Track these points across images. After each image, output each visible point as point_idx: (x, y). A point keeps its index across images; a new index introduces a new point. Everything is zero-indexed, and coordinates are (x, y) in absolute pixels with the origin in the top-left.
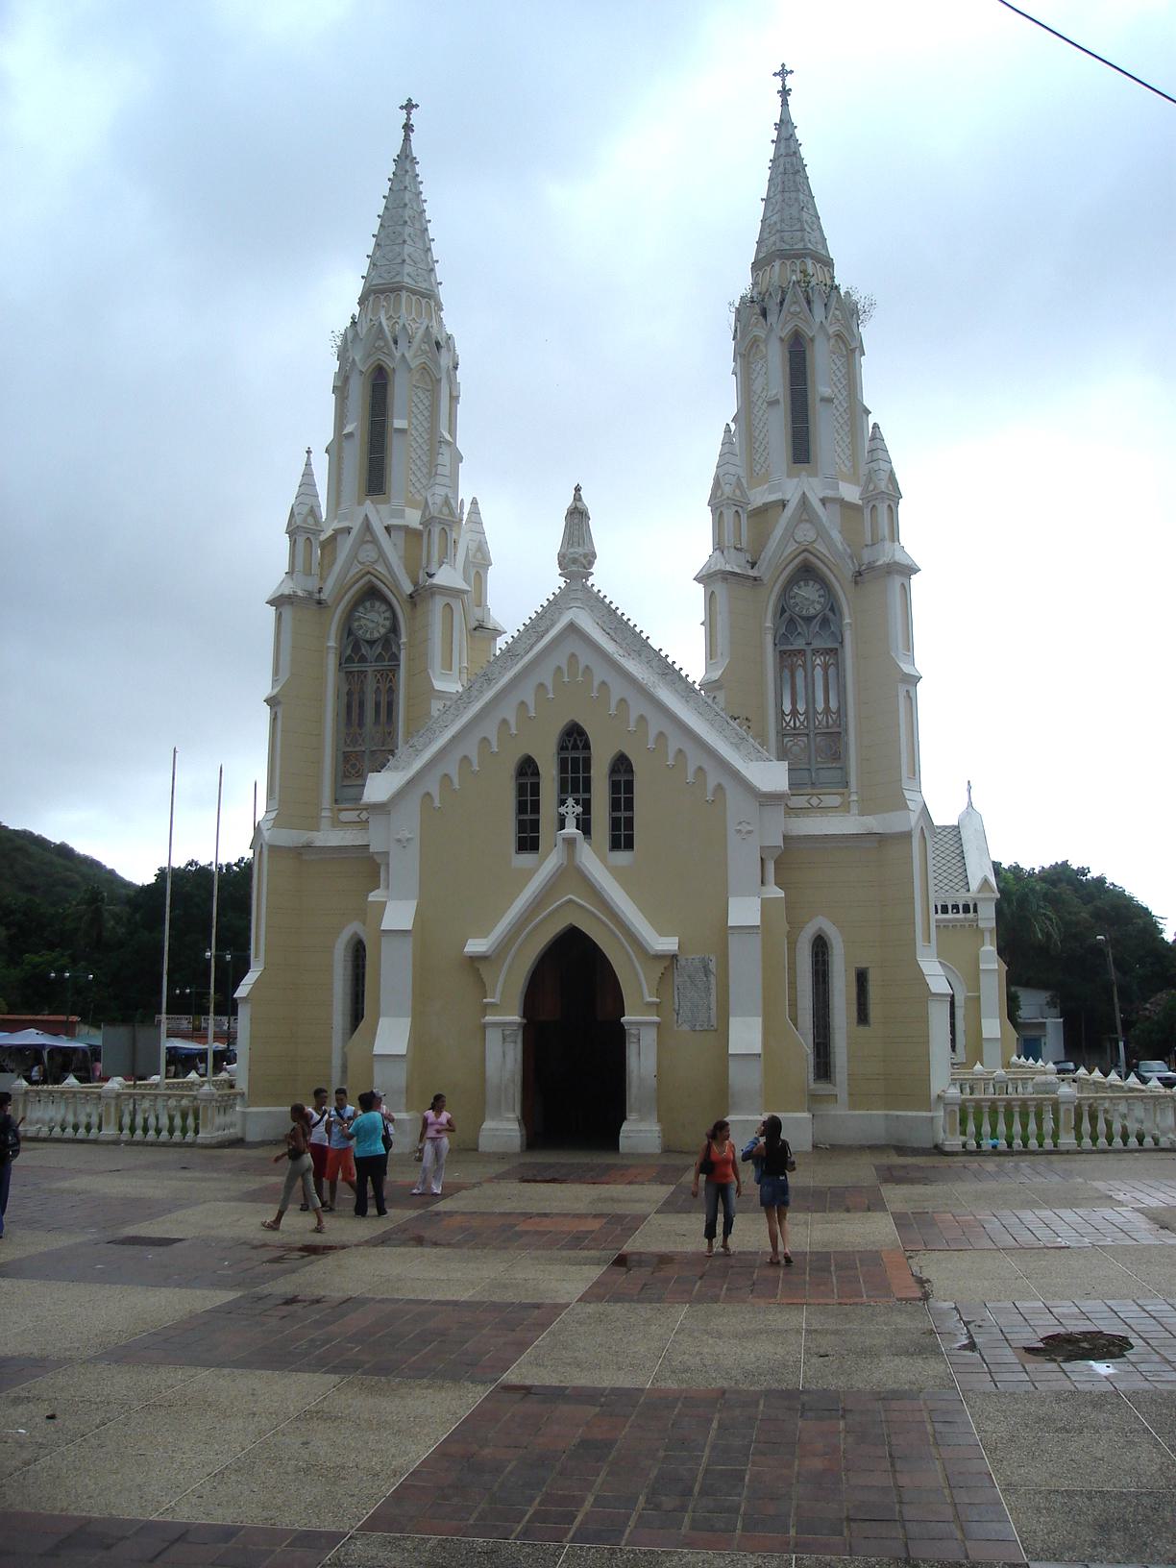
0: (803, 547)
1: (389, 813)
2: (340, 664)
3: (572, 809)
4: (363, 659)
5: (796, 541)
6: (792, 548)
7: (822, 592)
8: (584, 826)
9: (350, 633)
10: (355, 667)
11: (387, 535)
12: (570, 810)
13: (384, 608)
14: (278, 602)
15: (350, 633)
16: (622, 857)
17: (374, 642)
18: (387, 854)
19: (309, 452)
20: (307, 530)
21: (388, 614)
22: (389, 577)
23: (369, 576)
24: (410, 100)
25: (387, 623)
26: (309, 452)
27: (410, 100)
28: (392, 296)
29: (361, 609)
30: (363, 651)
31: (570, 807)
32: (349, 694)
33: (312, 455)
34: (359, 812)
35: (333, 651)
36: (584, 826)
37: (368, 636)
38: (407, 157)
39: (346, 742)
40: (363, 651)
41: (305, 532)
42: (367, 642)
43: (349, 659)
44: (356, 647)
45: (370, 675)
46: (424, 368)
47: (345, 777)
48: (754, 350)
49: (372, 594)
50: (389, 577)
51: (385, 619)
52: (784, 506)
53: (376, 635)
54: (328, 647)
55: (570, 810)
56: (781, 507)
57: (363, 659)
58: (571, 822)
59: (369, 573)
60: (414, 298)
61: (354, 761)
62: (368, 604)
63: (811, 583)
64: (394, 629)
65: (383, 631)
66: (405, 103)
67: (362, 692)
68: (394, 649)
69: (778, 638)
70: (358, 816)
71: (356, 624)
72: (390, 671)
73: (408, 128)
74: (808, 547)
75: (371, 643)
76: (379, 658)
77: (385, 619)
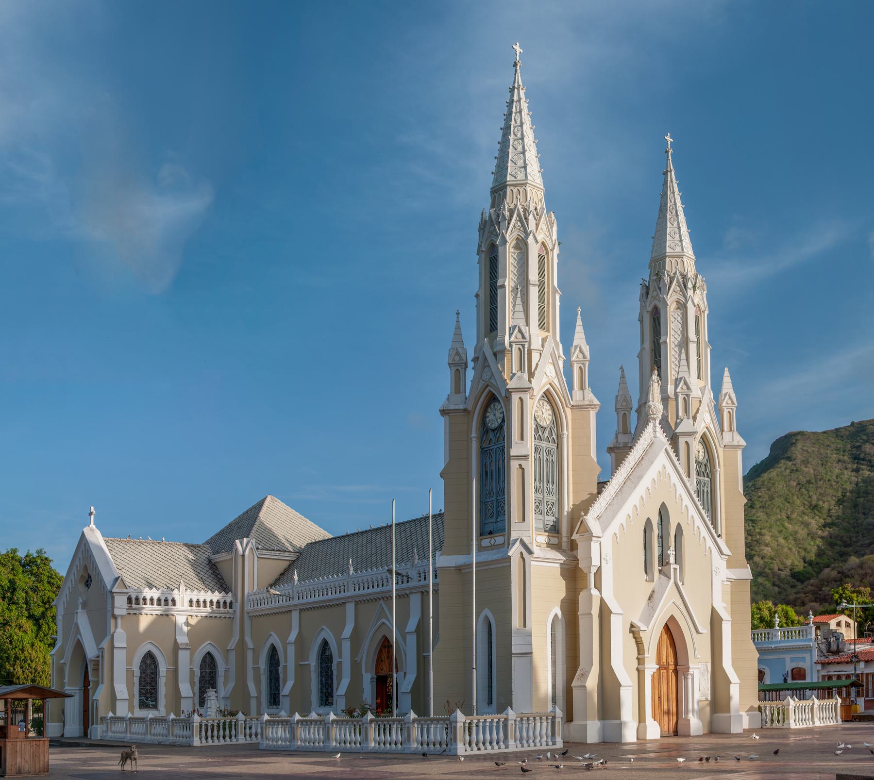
11: (495, 360)
14: (444, 412)
19: (458, 314)
23: (489, 387)
25: (501, 416)
26: (458, 314)
29: (489, 410)
33: (459, 316)
37: (493, 427)
40: (491, 437)
49: (492, 399)
53: (497, 425)
61: (489, 507)
64: (503, 421)
65: (500, 421)
75: (493, 430)
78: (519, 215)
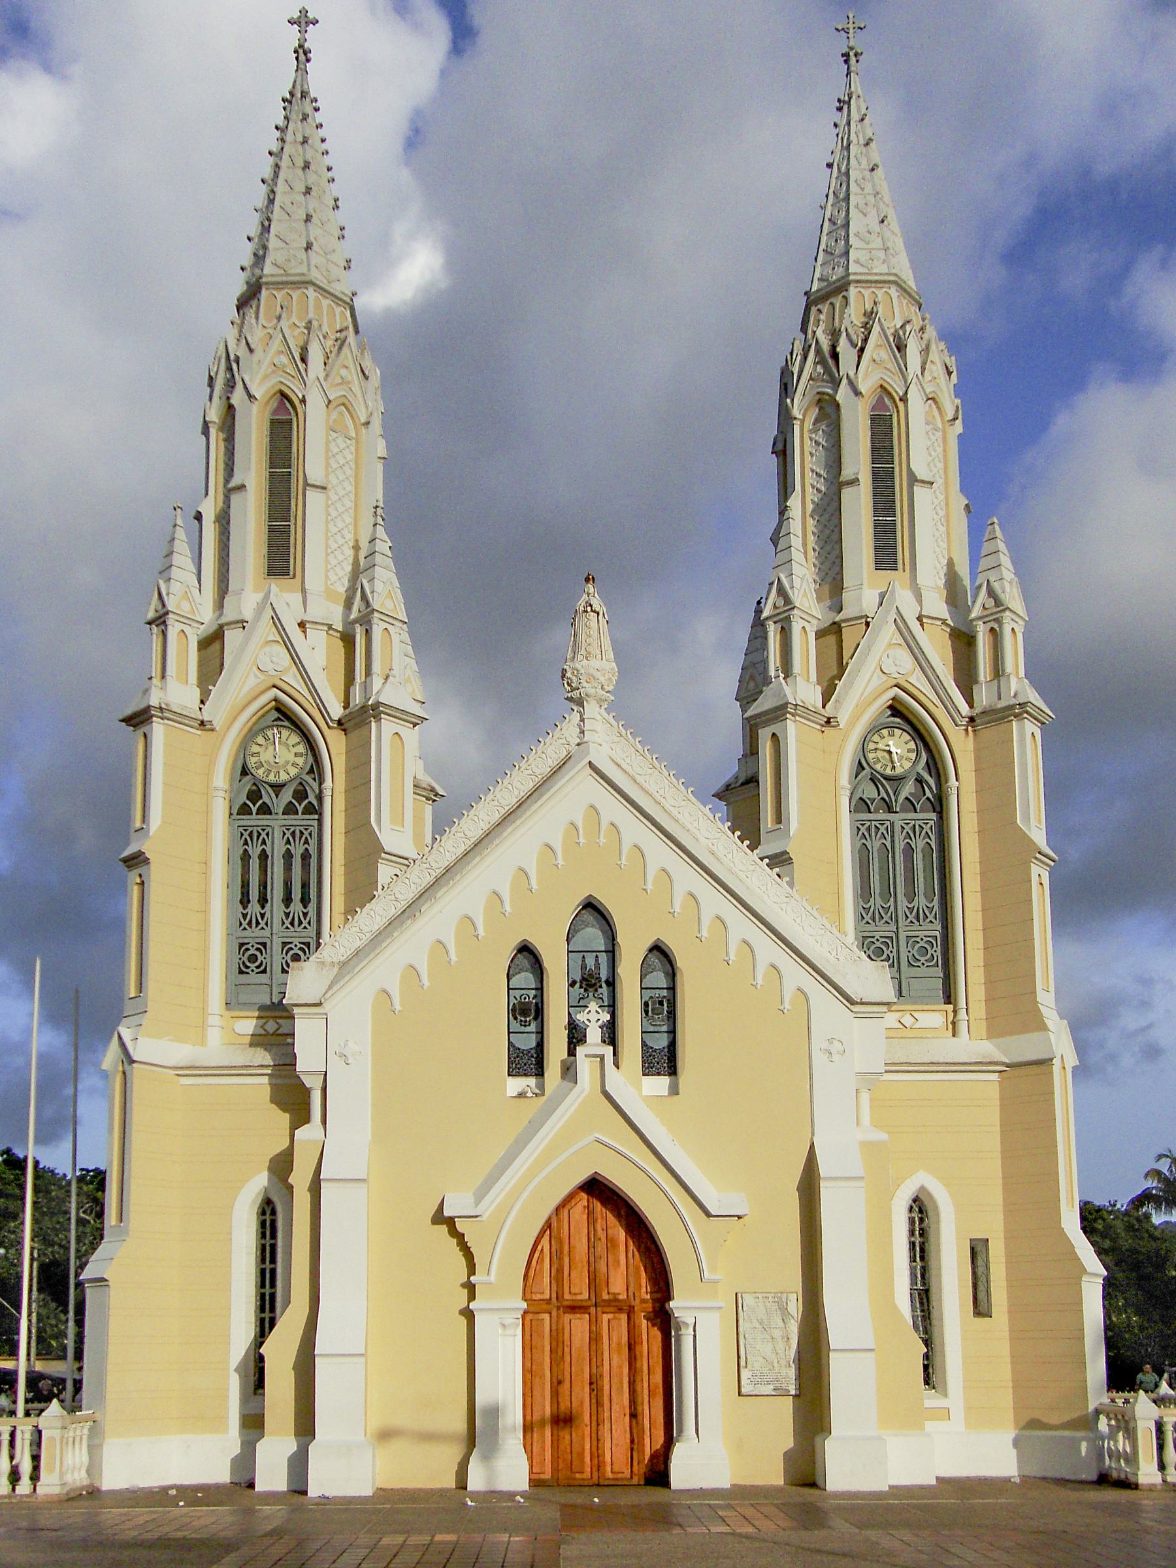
2: (231, 814)
3: (593, 1017)
4: (265, 810)
5: (881, 670)
7: (912, 745)
8: (611, 1034)
9: (245, 772)
10: (254, 820)
12: (593, 1017)
13: (295, 738)
15: (245, 772)
16: (661, 1083)
17: (283, 786)
21: (301, 748)
24: (304, 12)
27: (304, 12)
28: (296, 295)
29: (260, 740)
30: (265, 799)
31: (590, 1016)
32: (246, 857)
35: (222, 794)
36: (611, 1034)
37: (272, 778)
38: (304, 95)
40: (265, 799)
42: (271, 786)
43: (244, 810)
44: (254, 795)
45: (278, 834)
46: (344, 404)
47: (241, 972)
51: (296, 755)
53: (283, 777)
54: (216, 789)
55: (593, 1017)
57: (265, 810)
58: (594, 1035)
60: (326, 302)
63: (897, 732)
65: (293, 772)
66: (296, 15)
67: (264, 856)
68: (312, 798)
69: (853, 804)
70: (261, 1027)
71: (254, 760)
73: (302, 53)
75: (278, 788)
76: (290, 810)
77: (296, 755)
78: (819, 351)
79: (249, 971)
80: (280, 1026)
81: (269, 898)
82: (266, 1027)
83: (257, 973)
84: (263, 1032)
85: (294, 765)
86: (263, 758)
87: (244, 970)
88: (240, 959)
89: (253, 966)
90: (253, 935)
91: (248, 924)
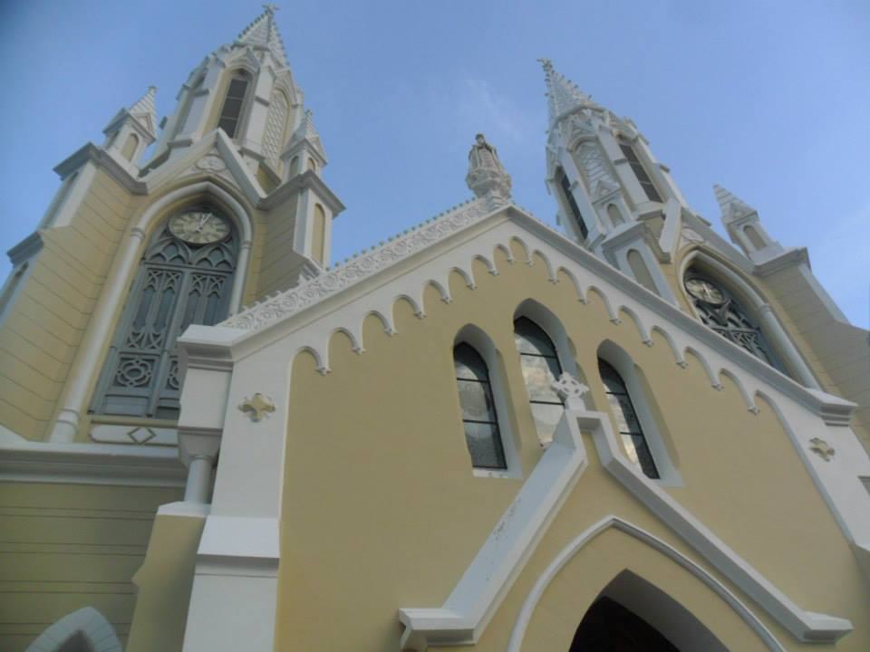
0: (693, 246)
1: (229, 368)
2: (143, 258)
6: (682, 244)
9: (167, 232)
18: (221, 431)
20: (136, 124)
22: (235, 183)
34: (134, 428)
37: (191, 240)
39: (129, 341)
41: (134, 127)
47: (117, 383)
48: (580, 148)
50: (235, 183)
52: (664, 217)
53: (202, 241)
56: (660, 218)
59: (209, 179)
62: (197, 215)
64: (233, 235)
72: (218, 277)
74: (701, 245)
79: (127, 383)
80: (153, 435)
81: (167, 322)
82: (134, 435)
83: (137, 386)
84: (131, 440)
85: (214, 235)
86: (185, 228)
87: (122, 382)
88: (119, 372)
89: (132, 379)
90: (139, 351)
91: (137, 343)
